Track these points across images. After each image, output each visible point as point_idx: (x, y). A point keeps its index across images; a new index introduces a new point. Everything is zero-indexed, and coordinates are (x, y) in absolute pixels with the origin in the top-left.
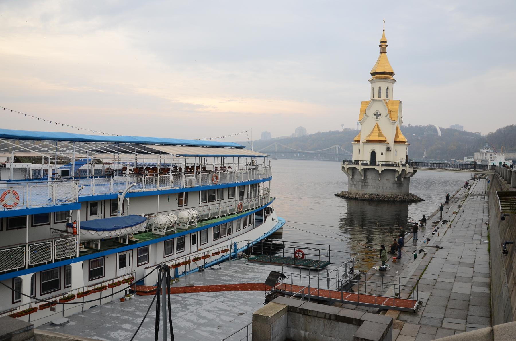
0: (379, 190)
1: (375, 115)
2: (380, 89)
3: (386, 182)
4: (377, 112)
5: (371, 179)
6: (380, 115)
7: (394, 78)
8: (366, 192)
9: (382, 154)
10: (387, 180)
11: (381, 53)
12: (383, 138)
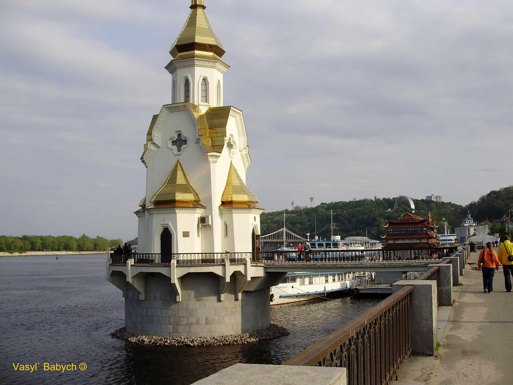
1: (174, 143)
4: (179, 135)
5: (158, 299)
6: (185, 142)
9: (186, 234)
12: (190, 194)
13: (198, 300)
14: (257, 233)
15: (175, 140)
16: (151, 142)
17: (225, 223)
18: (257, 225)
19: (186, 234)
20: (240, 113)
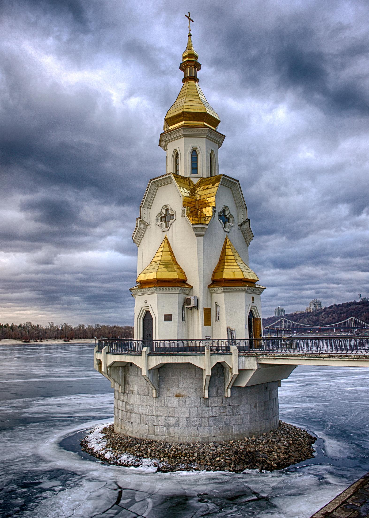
0: (158, 429)
2: (176, 155)
3: (173, 402)
4: (167, 210)
5: (136, 392)
7: (220, 129)
8: (129, 434)
9: (168, 318)
10: (177, 396)
11: (185, 80)
13: (178, 397)
14: (257, 316)
15: (163, 215)
16: (139, 220)
17: (216, 305)
18: (256, 306)
19: (168, 318)
20: (236, 183)
